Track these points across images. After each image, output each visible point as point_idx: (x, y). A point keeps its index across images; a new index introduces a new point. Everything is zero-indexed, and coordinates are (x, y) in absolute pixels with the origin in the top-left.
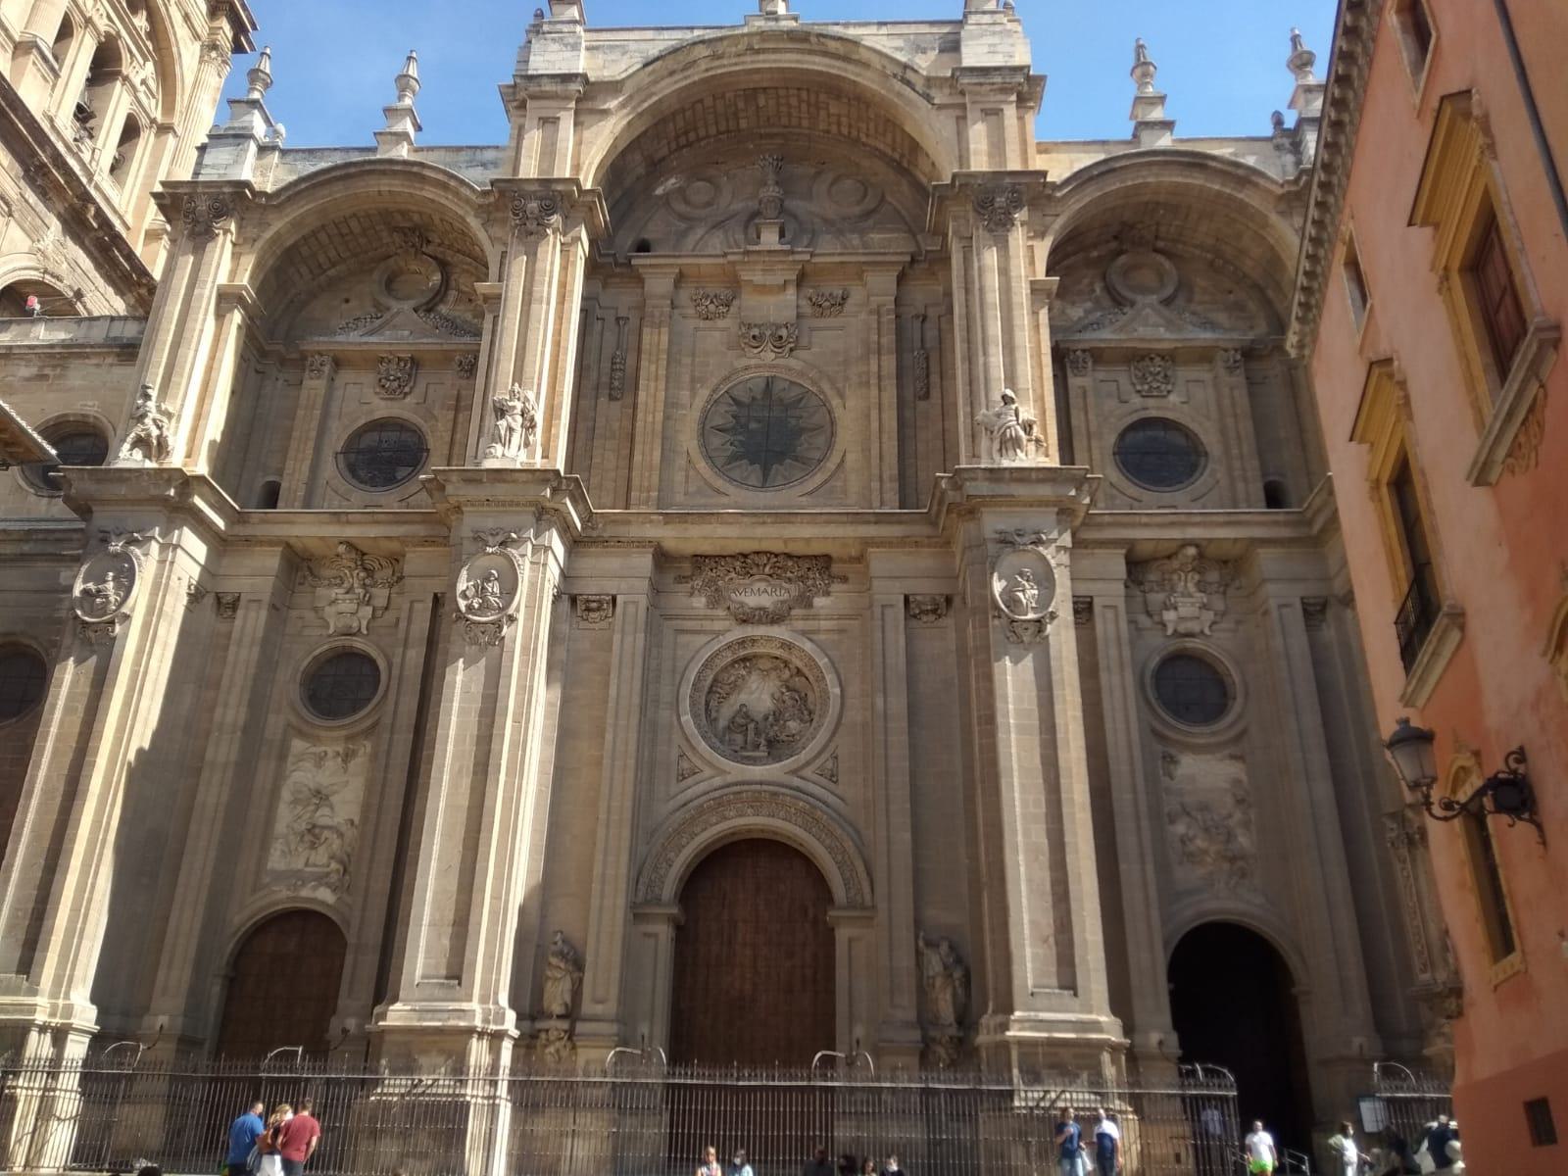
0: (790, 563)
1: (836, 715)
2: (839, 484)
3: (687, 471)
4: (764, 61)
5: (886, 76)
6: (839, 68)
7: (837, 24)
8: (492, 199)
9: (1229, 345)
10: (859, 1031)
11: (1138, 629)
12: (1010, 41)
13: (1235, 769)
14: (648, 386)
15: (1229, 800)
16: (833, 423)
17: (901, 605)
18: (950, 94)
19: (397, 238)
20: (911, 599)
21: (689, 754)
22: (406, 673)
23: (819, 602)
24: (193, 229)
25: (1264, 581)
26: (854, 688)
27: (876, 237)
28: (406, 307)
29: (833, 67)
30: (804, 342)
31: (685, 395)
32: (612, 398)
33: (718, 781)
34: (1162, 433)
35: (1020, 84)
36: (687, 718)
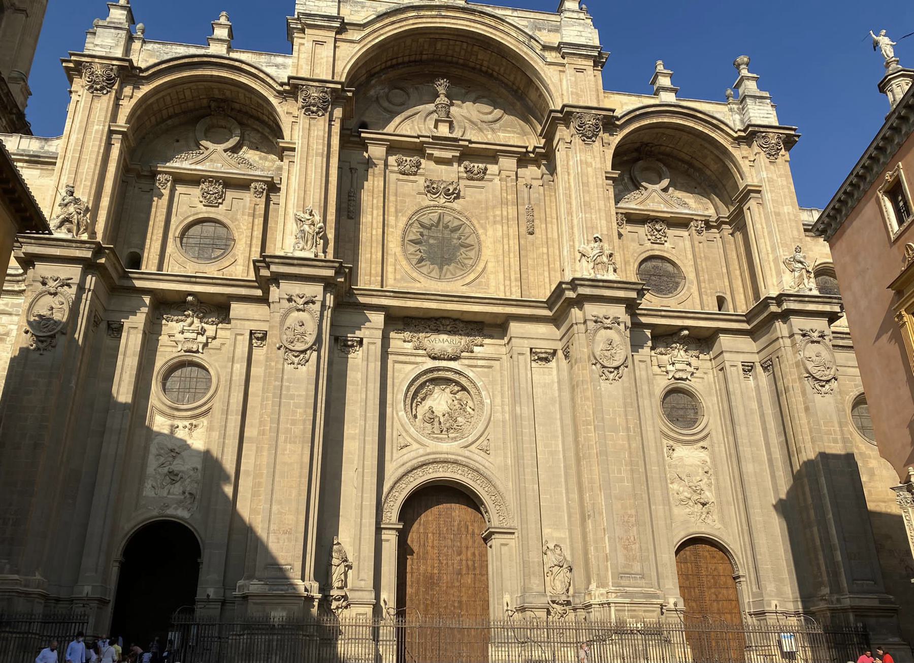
0: (461, 325)
1: (488, 416)
2: (483, 280)
3: (395, 265)
4: (447, 23)
5: (519, 41)
6: (491, 33)
7: (489, 7)
8: (287, 88)
9: (699, 218)
10: (507, 598)
11: (654, 375)
12: (589, 30)
13: (704, 455)
14: (372, 212)
15: (700, 470)
16: (479, 243)
17: (528, 353)
18: (556, 57)
19: (213, 105)
20: (534, 350)
21: (404, 434)
22: (234, 378)
23: (476, 349)
24: (91, 87)
25: (722, 353)
26: (498, 400)
27: (501, 135)
28: (219, 148)
29: (488, 32)
30: (462, 194)
31: (391, 220)
32: (350, 218)
33: (421, 451)
34: (661, 264)
35: (595, 56)
36: (402, 413)
